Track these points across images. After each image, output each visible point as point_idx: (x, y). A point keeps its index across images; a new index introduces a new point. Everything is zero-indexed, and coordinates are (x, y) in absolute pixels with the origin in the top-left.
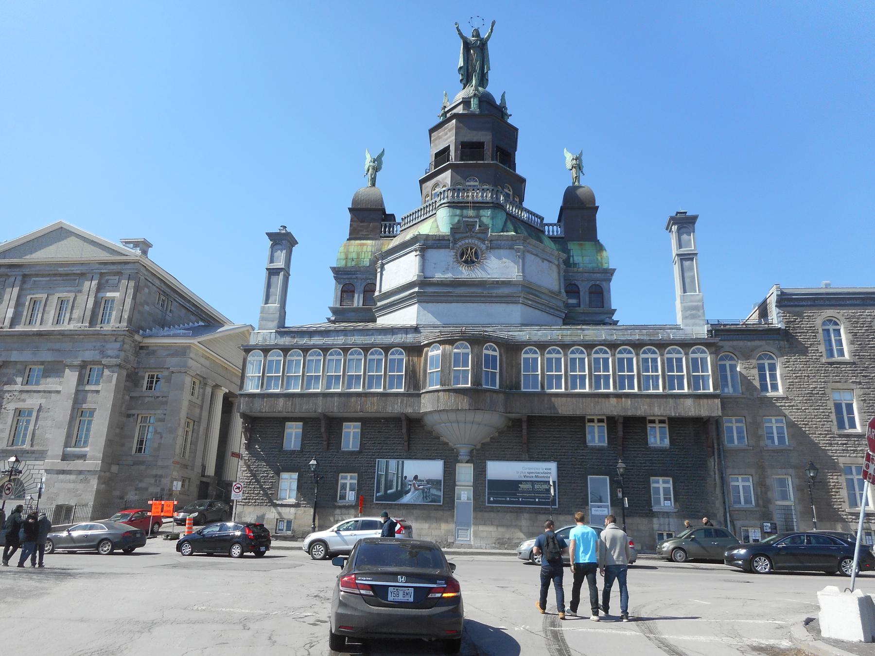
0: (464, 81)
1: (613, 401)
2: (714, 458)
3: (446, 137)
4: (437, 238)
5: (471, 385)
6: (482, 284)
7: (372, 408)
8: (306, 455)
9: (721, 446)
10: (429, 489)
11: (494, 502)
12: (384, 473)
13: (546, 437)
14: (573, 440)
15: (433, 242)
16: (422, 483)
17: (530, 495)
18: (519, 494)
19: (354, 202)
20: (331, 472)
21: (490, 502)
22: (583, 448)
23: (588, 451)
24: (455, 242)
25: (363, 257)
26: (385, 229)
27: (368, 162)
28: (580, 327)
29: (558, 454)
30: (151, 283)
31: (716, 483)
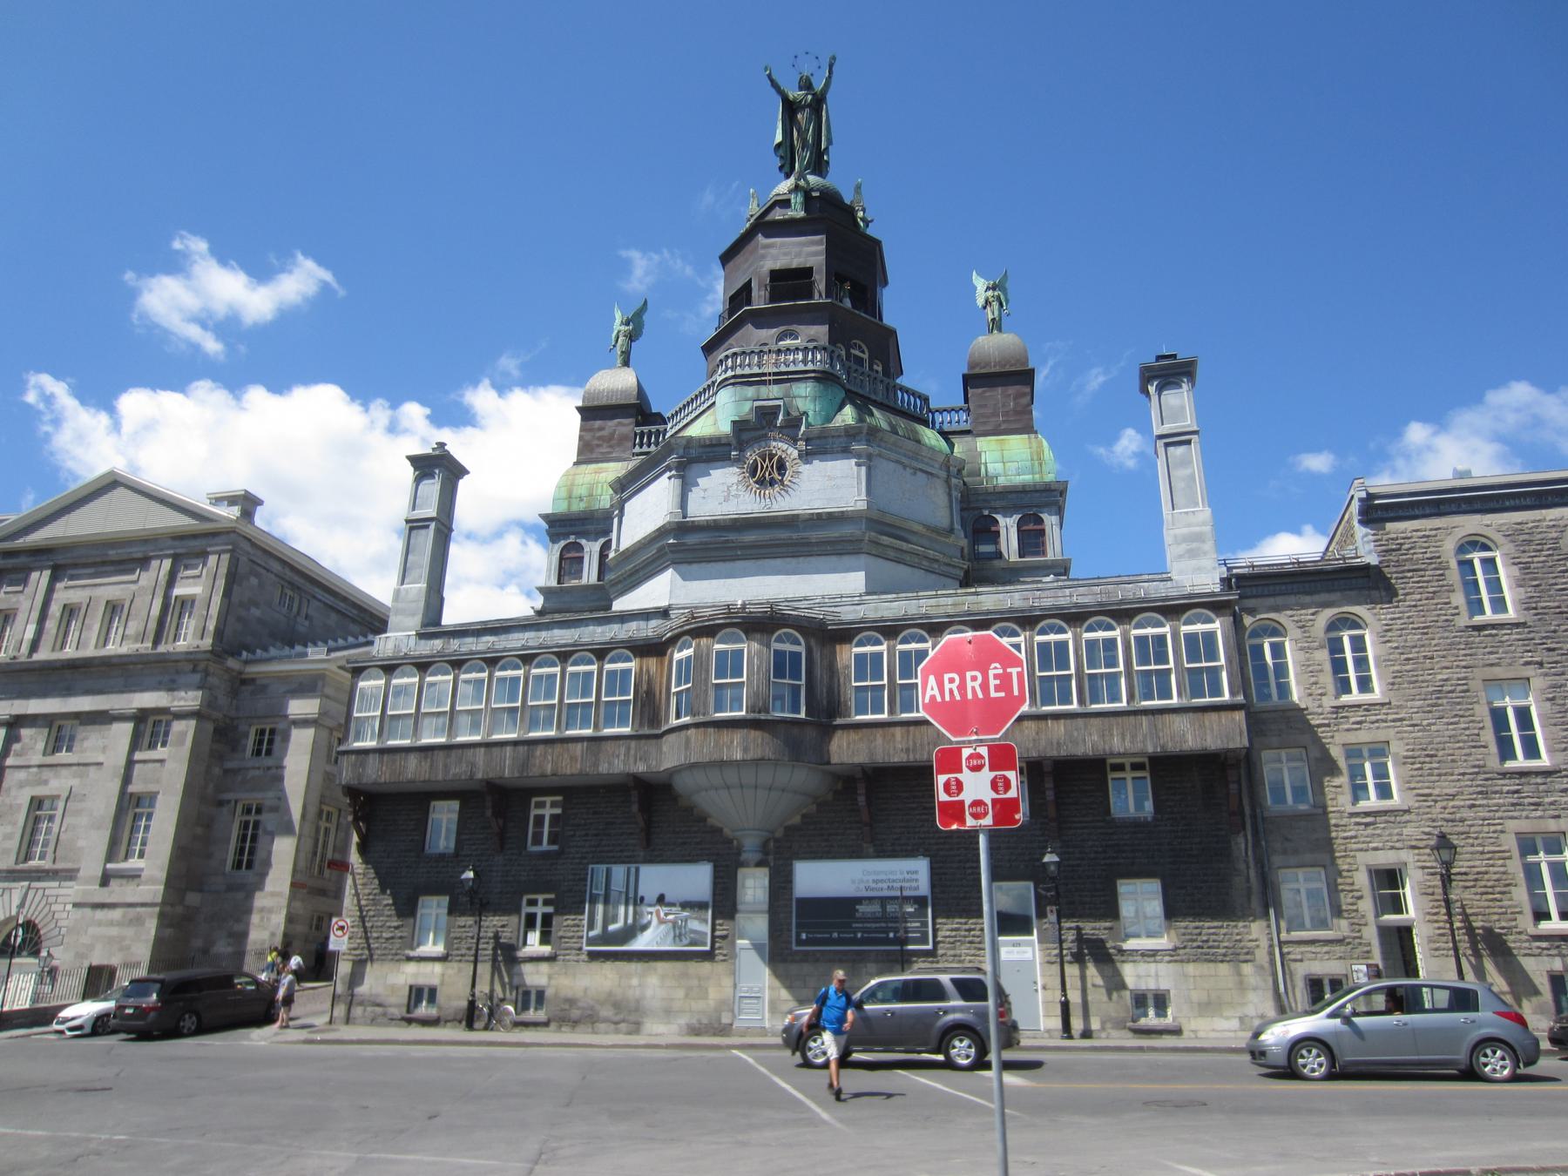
2: (1246, 836)
3: (746, 266)
4: (708, 442)
5: (747, 712)
7: (570, 765)
9: (1258, 811)
10: (686, 921)
12: (603, 892)
15: (701, 450)
17: (878, 925)
18: (857, 925)
21: (800, 942)
24: (741, 448)
25: (599, 491)
26: (641, 439)
28: (973, 590)
29: (933, 841)
30: (265, 568)
31: (1249, 888)
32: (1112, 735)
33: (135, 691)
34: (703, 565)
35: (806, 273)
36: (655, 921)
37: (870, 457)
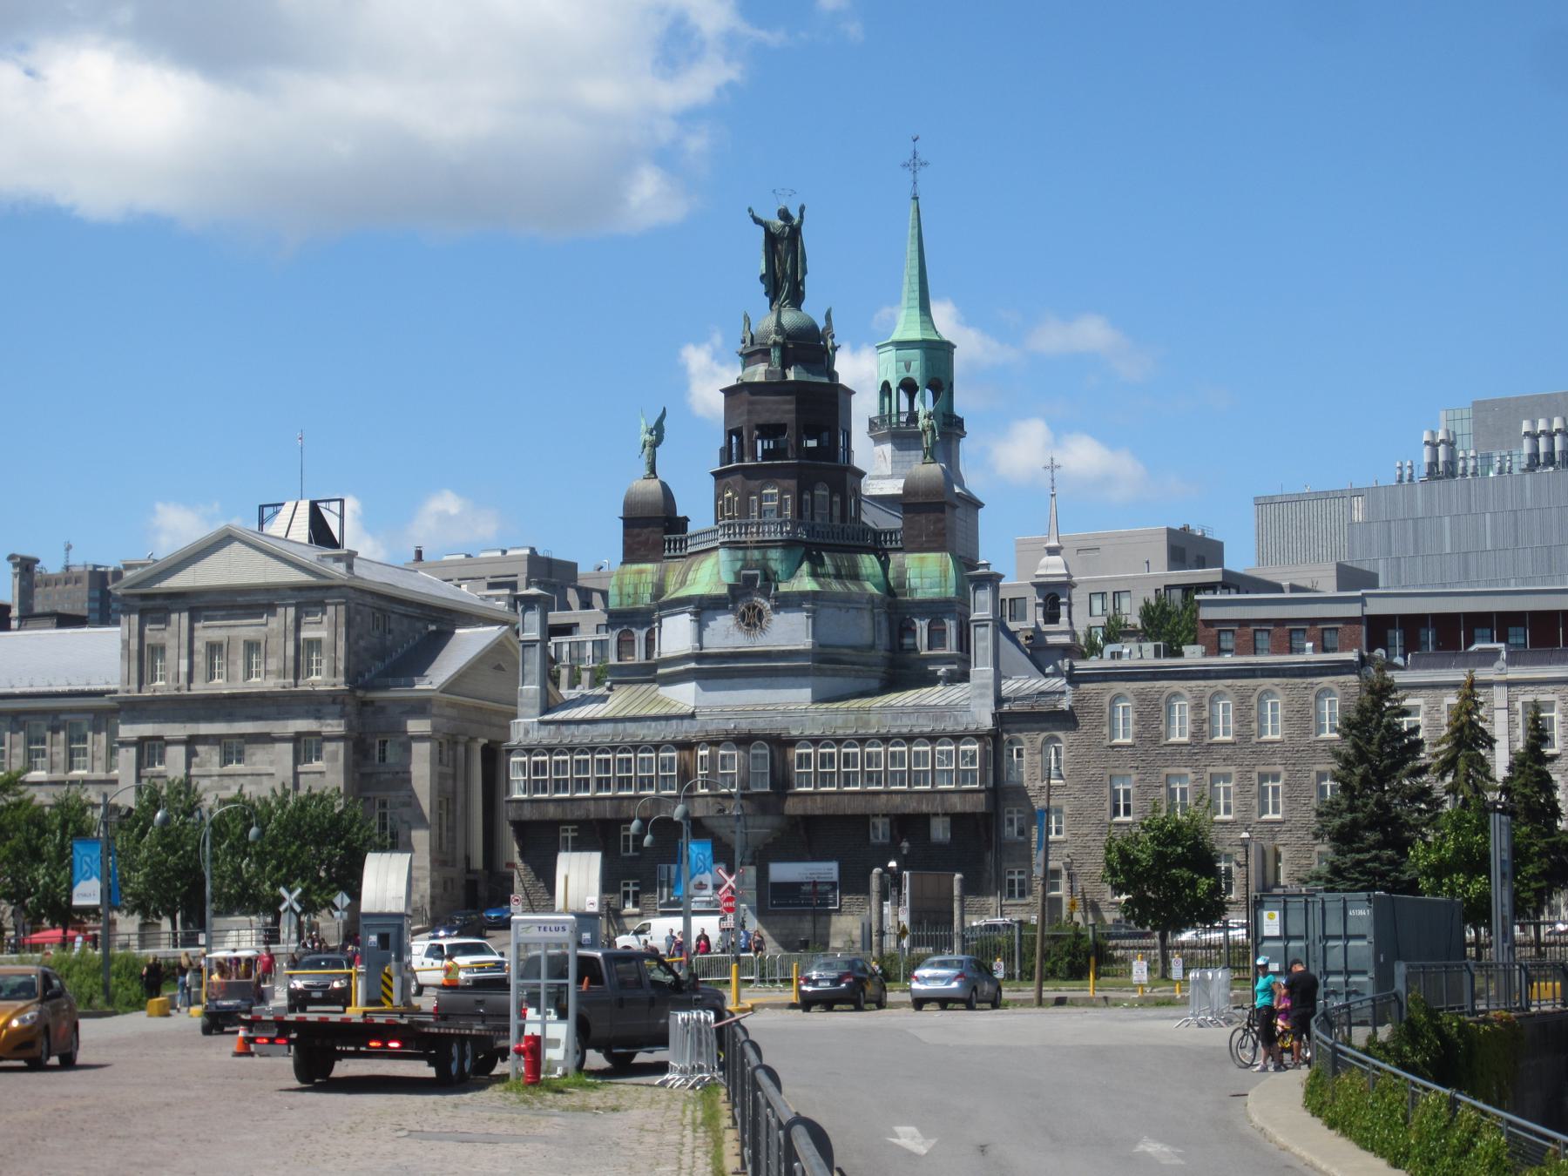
1: (884, 797)
19: (628, 506)
21: (772, 905)
33: (288, 719)
37: (814, 612)
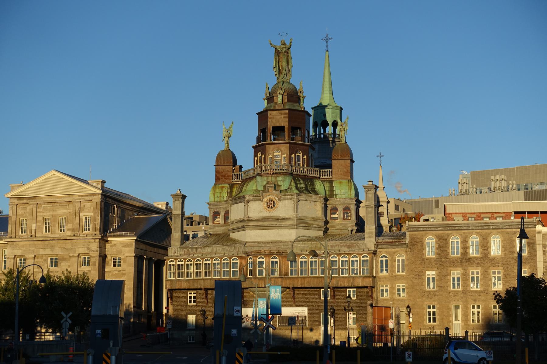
0: (278, 76)
6: (277, 219)
8: (198, 307)
9: (377, 298)
11: (281, 326)
13: (304, 296)
14: (315, 297)
16: (250, 318)
20: (210, 314)
21: (279, 326)
22: (319, 300)
23: (321, 302)
27: (224, 133)
29: (308, 303)
32: (345, 282)
34: (254, 231)
35: (284, 127)
36: (246, 321)
